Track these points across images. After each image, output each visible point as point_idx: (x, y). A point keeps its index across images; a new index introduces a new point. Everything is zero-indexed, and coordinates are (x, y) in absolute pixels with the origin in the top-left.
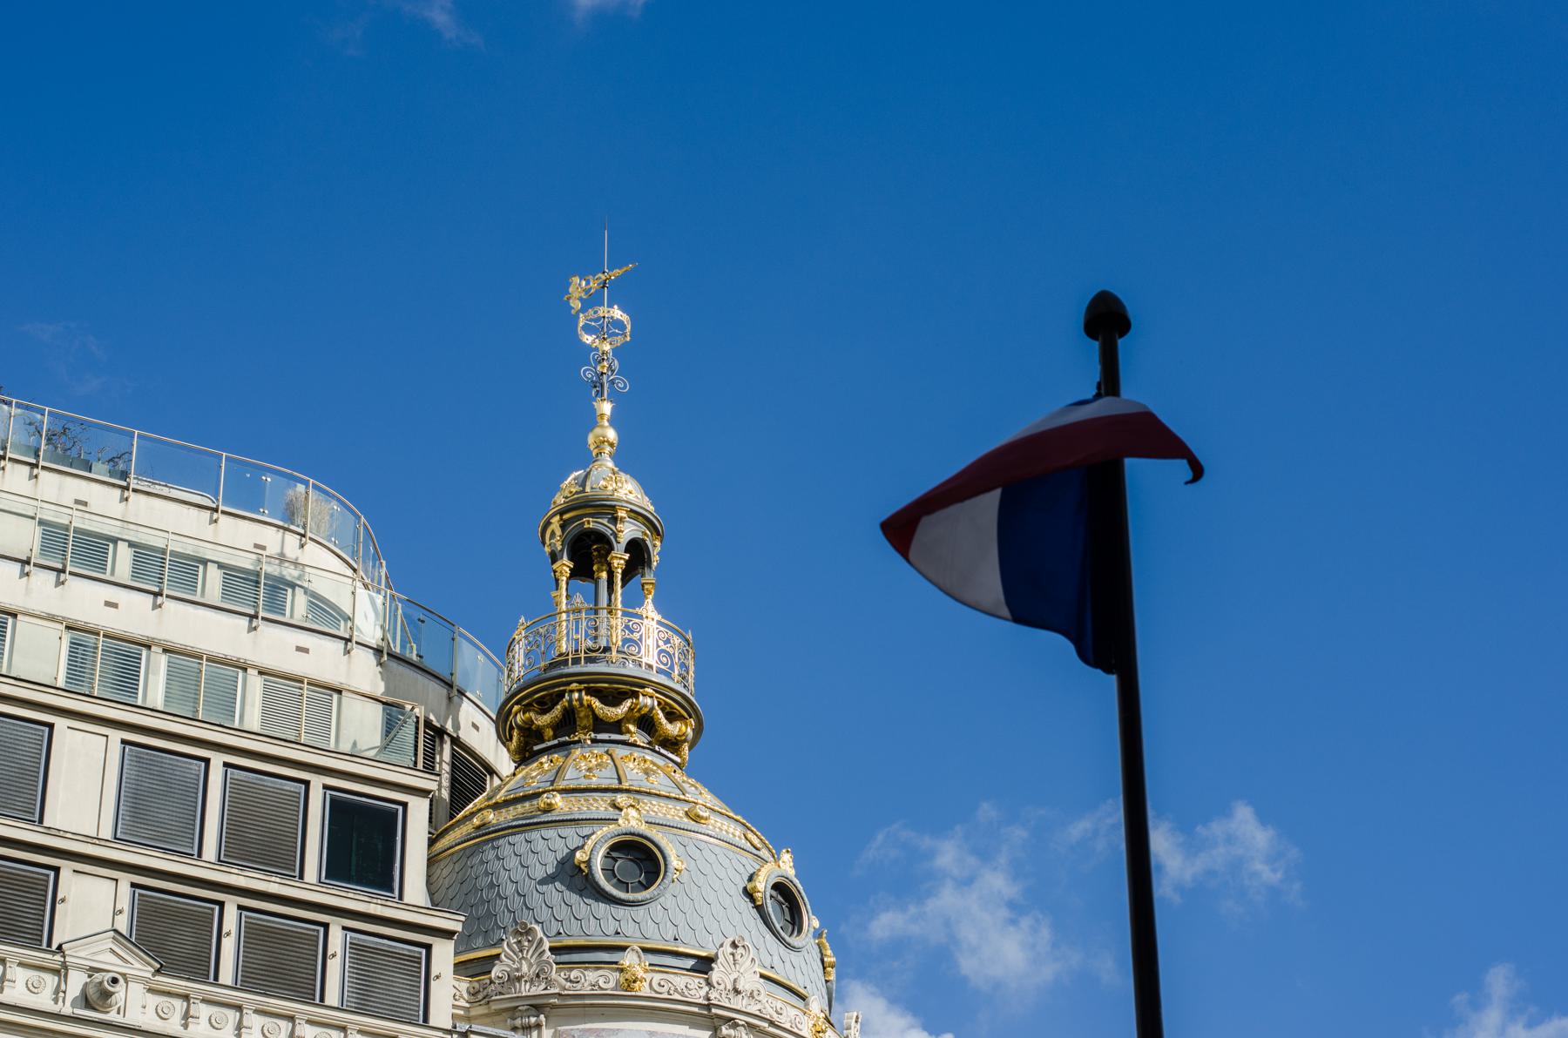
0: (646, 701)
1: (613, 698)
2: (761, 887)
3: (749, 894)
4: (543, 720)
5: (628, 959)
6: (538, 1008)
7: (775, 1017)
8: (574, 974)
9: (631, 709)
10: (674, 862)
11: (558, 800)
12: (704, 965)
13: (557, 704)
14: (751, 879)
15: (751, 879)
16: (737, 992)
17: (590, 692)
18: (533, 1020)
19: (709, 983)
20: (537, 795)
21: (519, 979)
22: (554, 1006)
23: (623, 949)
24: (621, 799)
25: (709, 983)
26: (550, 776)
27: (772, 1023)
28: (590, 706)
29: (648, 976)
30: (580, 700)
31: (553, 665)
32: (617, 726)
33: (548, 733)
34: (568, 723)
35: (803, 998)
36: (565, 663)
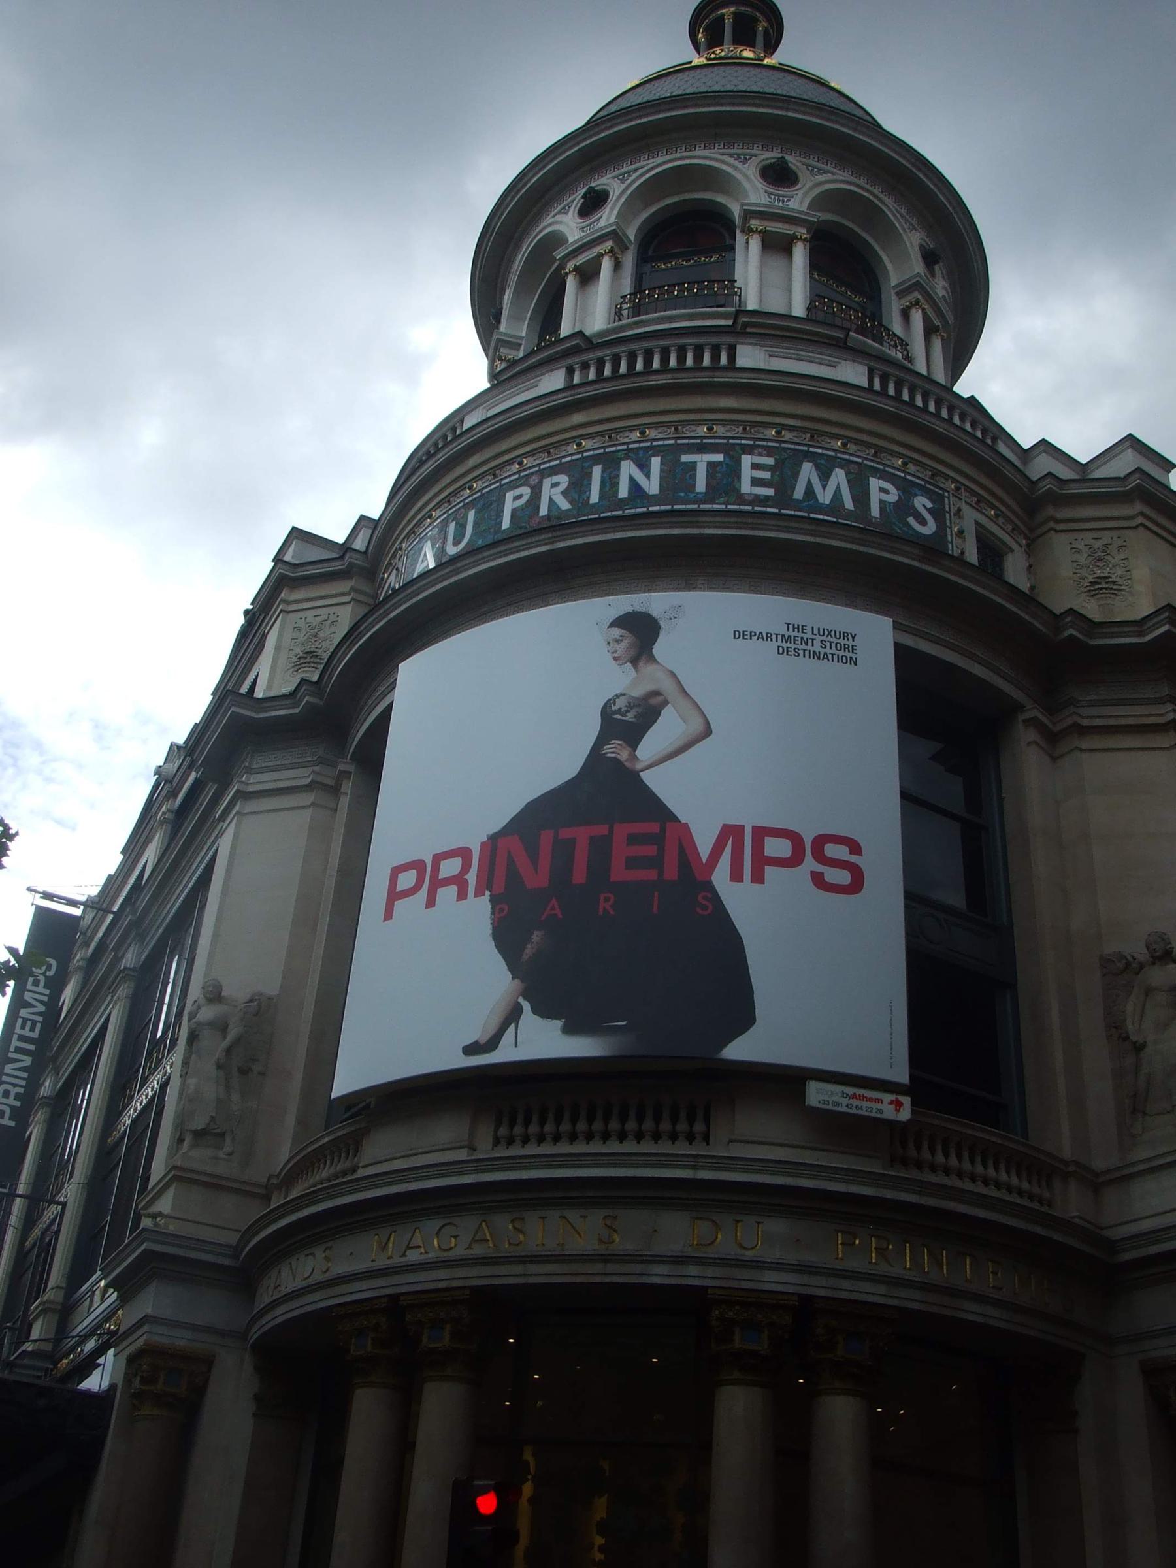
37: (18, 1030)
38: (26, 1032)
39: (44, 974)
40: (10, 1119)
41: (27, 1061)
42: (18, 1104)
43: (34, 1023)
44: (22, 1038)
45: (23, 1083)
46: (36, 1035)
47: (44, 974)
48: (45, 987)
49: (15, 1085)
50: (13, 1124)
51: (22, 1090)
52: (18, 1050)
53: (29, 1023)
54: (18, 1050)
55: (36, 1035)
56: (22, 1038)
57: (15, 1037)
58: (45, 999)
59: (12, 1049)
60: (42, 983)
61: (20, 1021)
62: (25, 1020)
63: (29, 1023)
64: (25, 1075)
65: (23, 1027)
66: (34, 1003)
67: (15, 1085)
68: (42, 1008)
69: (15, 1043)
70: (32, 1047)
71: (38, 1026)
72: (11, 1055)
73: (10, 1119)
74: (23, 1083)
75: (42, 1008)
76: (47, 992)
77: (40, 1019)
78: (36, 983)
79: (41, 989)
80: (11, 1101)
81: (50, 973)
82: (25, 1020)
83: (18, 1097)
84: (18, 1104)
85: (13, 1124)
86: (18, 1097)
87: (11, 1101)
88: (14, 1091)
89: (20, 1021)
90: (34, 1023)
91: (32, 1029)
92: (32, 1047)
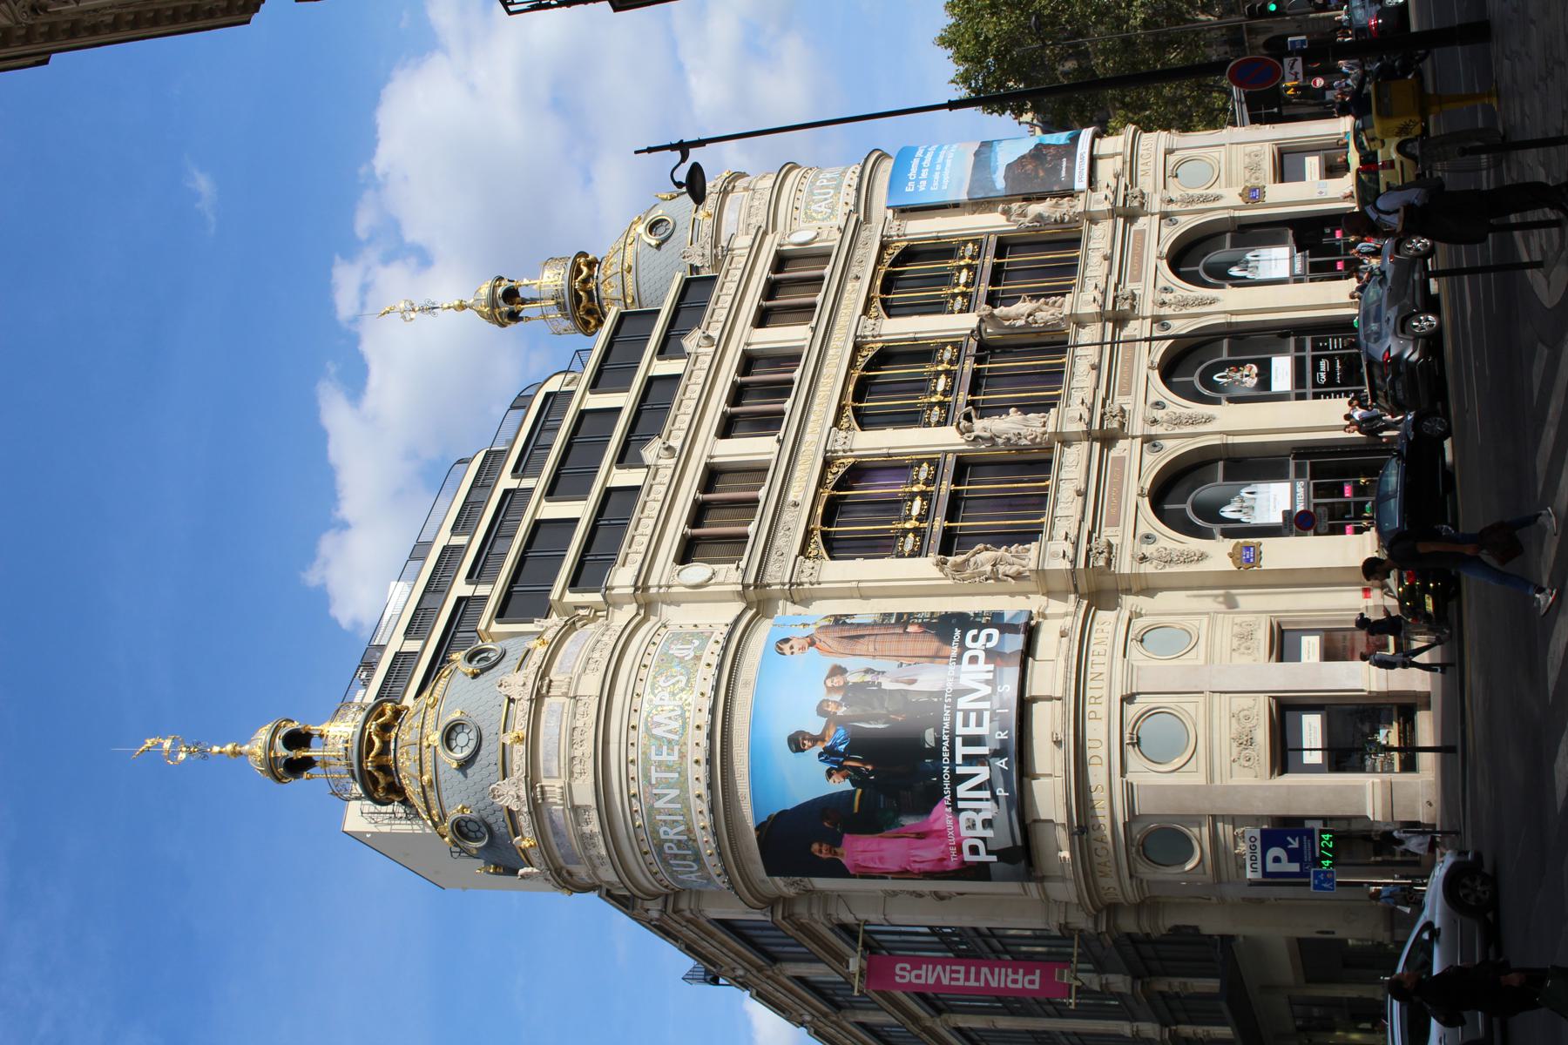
0: (372, 726)
1: (371, 743)
2: (471, 670)
3: (475, 676)
4: (382, 782)
5: (508, 742)
6: (533, 788)
7: (537, 665)
8: (515, 768)
9: (377, 736)
10: (456, 715)
11: (426, 778)
12: (511, 700)
13: (374, 776)
14: (466, 675)
15: (466, 675)
16: (524, 684)
17: (367, 758)
18: (538, 789)
19: (520, 700)
20: (423, 787)
21: (518, 797)
22: (531, 780)
23: (504, 744)
24: (425, 744)
25: (520, 700)
26: (414, 781)
27: (540, 667)
28: (374, 757)
29: (516, 730)
30: (371, 762)
31: (353, 777)
32: (385, 744)
33: (390, 779)
34: (384, 769)
35: (529, 651)
36: (352, 771)
37: (961, 983)
38: (962, 976)
39: (910, 972)
40: (1034, 974)
41: (985, 970)
42: (1021, 971)
43: (952, 972)
44: (967, 979)
45: (1003, 970)
46: (962, 969)
47: (910, 972)
48: (920, 969)
49: (1007, 976)
50: (1038, 972)
51: (1010, 970)
52: (977, 979)
53: (954, 975)
54: (977, 979)
55: (962, 969)
56: (967, 979)
57: (967, 984)
58: (930, 967)
59: (977, 984)
60: (918, 972)
61: (953, 983)
62: (951, 979)
63: (954, 975)
64: (997, 970)
65: (958, 979)
66: (935, 975)
67: (1007, 976)
68: (939, 968)
69: (972, 983)
70: (973, 969)
71: (954, 968)
72: (982, 984)
73: (1034, 974)
74: (1003, 970)
75: (939, 968)
76: (924, 967)
77: (948, 968)
78: (918, 977)
79: (923, 972)
80: (1020, 977)
81: (908, 967)
82: (951, 979)
83: (1015, 972)
84: (1021, 971)
85: (1038, 972)
86: (1015, 972)
87: (1020, 977)
88: (1011, 976)
89: (953, 983)
90: (952, 972)
91: (958, 972)
92: (973, 969)
